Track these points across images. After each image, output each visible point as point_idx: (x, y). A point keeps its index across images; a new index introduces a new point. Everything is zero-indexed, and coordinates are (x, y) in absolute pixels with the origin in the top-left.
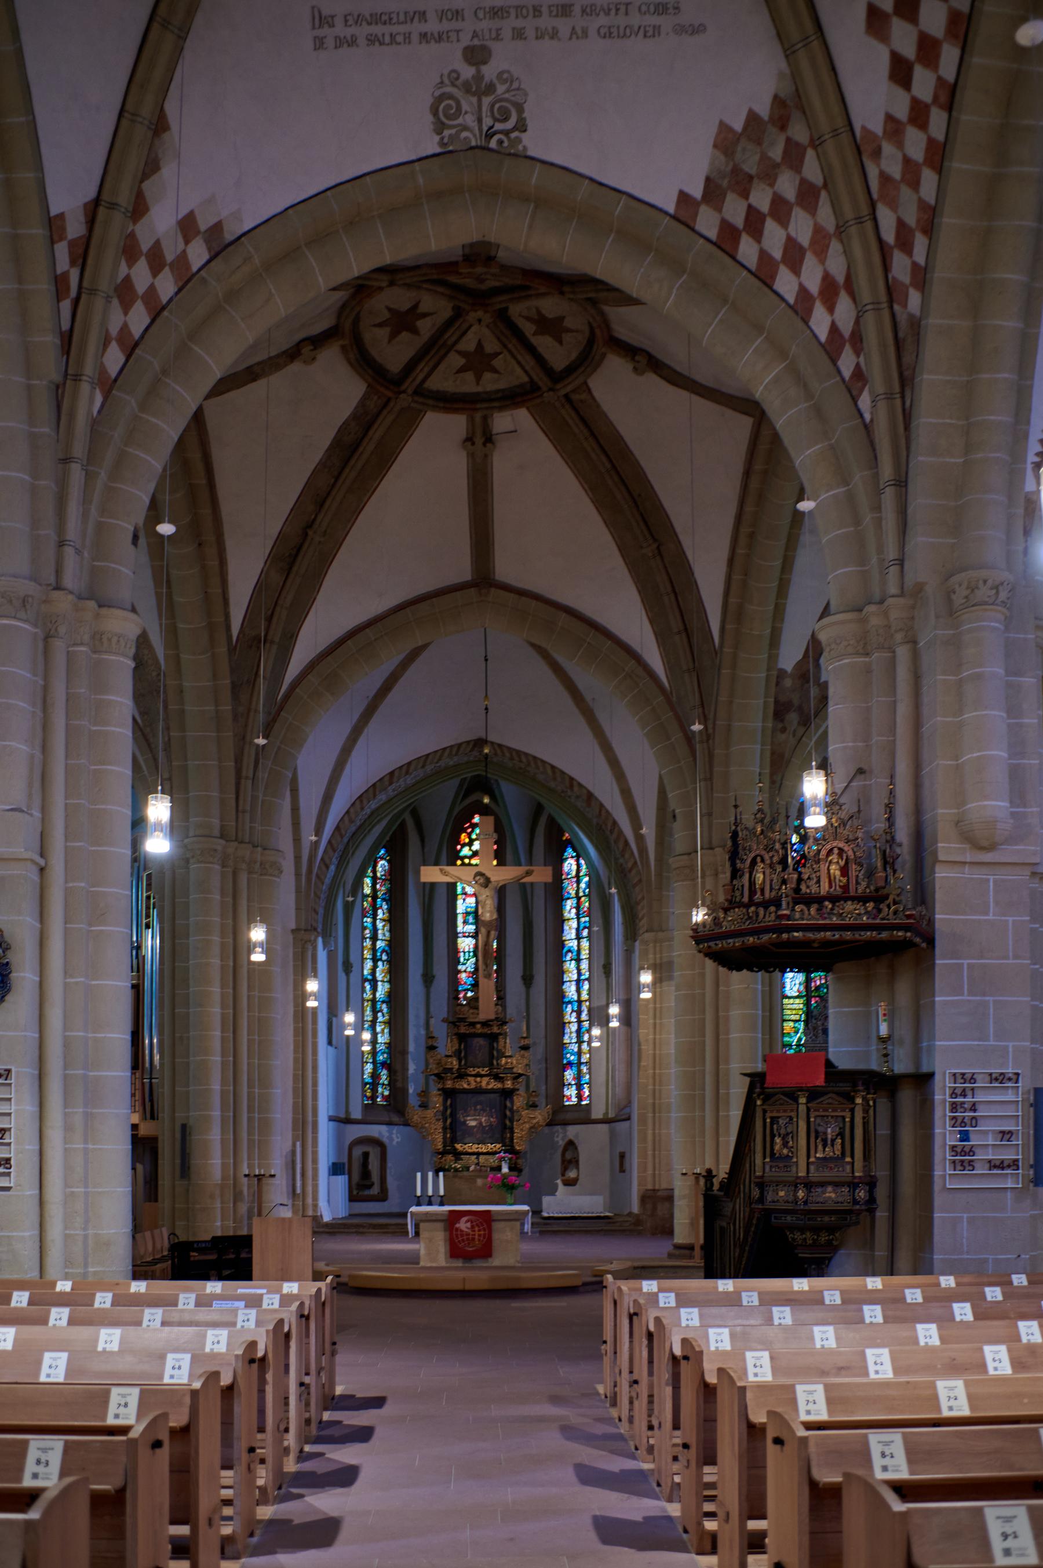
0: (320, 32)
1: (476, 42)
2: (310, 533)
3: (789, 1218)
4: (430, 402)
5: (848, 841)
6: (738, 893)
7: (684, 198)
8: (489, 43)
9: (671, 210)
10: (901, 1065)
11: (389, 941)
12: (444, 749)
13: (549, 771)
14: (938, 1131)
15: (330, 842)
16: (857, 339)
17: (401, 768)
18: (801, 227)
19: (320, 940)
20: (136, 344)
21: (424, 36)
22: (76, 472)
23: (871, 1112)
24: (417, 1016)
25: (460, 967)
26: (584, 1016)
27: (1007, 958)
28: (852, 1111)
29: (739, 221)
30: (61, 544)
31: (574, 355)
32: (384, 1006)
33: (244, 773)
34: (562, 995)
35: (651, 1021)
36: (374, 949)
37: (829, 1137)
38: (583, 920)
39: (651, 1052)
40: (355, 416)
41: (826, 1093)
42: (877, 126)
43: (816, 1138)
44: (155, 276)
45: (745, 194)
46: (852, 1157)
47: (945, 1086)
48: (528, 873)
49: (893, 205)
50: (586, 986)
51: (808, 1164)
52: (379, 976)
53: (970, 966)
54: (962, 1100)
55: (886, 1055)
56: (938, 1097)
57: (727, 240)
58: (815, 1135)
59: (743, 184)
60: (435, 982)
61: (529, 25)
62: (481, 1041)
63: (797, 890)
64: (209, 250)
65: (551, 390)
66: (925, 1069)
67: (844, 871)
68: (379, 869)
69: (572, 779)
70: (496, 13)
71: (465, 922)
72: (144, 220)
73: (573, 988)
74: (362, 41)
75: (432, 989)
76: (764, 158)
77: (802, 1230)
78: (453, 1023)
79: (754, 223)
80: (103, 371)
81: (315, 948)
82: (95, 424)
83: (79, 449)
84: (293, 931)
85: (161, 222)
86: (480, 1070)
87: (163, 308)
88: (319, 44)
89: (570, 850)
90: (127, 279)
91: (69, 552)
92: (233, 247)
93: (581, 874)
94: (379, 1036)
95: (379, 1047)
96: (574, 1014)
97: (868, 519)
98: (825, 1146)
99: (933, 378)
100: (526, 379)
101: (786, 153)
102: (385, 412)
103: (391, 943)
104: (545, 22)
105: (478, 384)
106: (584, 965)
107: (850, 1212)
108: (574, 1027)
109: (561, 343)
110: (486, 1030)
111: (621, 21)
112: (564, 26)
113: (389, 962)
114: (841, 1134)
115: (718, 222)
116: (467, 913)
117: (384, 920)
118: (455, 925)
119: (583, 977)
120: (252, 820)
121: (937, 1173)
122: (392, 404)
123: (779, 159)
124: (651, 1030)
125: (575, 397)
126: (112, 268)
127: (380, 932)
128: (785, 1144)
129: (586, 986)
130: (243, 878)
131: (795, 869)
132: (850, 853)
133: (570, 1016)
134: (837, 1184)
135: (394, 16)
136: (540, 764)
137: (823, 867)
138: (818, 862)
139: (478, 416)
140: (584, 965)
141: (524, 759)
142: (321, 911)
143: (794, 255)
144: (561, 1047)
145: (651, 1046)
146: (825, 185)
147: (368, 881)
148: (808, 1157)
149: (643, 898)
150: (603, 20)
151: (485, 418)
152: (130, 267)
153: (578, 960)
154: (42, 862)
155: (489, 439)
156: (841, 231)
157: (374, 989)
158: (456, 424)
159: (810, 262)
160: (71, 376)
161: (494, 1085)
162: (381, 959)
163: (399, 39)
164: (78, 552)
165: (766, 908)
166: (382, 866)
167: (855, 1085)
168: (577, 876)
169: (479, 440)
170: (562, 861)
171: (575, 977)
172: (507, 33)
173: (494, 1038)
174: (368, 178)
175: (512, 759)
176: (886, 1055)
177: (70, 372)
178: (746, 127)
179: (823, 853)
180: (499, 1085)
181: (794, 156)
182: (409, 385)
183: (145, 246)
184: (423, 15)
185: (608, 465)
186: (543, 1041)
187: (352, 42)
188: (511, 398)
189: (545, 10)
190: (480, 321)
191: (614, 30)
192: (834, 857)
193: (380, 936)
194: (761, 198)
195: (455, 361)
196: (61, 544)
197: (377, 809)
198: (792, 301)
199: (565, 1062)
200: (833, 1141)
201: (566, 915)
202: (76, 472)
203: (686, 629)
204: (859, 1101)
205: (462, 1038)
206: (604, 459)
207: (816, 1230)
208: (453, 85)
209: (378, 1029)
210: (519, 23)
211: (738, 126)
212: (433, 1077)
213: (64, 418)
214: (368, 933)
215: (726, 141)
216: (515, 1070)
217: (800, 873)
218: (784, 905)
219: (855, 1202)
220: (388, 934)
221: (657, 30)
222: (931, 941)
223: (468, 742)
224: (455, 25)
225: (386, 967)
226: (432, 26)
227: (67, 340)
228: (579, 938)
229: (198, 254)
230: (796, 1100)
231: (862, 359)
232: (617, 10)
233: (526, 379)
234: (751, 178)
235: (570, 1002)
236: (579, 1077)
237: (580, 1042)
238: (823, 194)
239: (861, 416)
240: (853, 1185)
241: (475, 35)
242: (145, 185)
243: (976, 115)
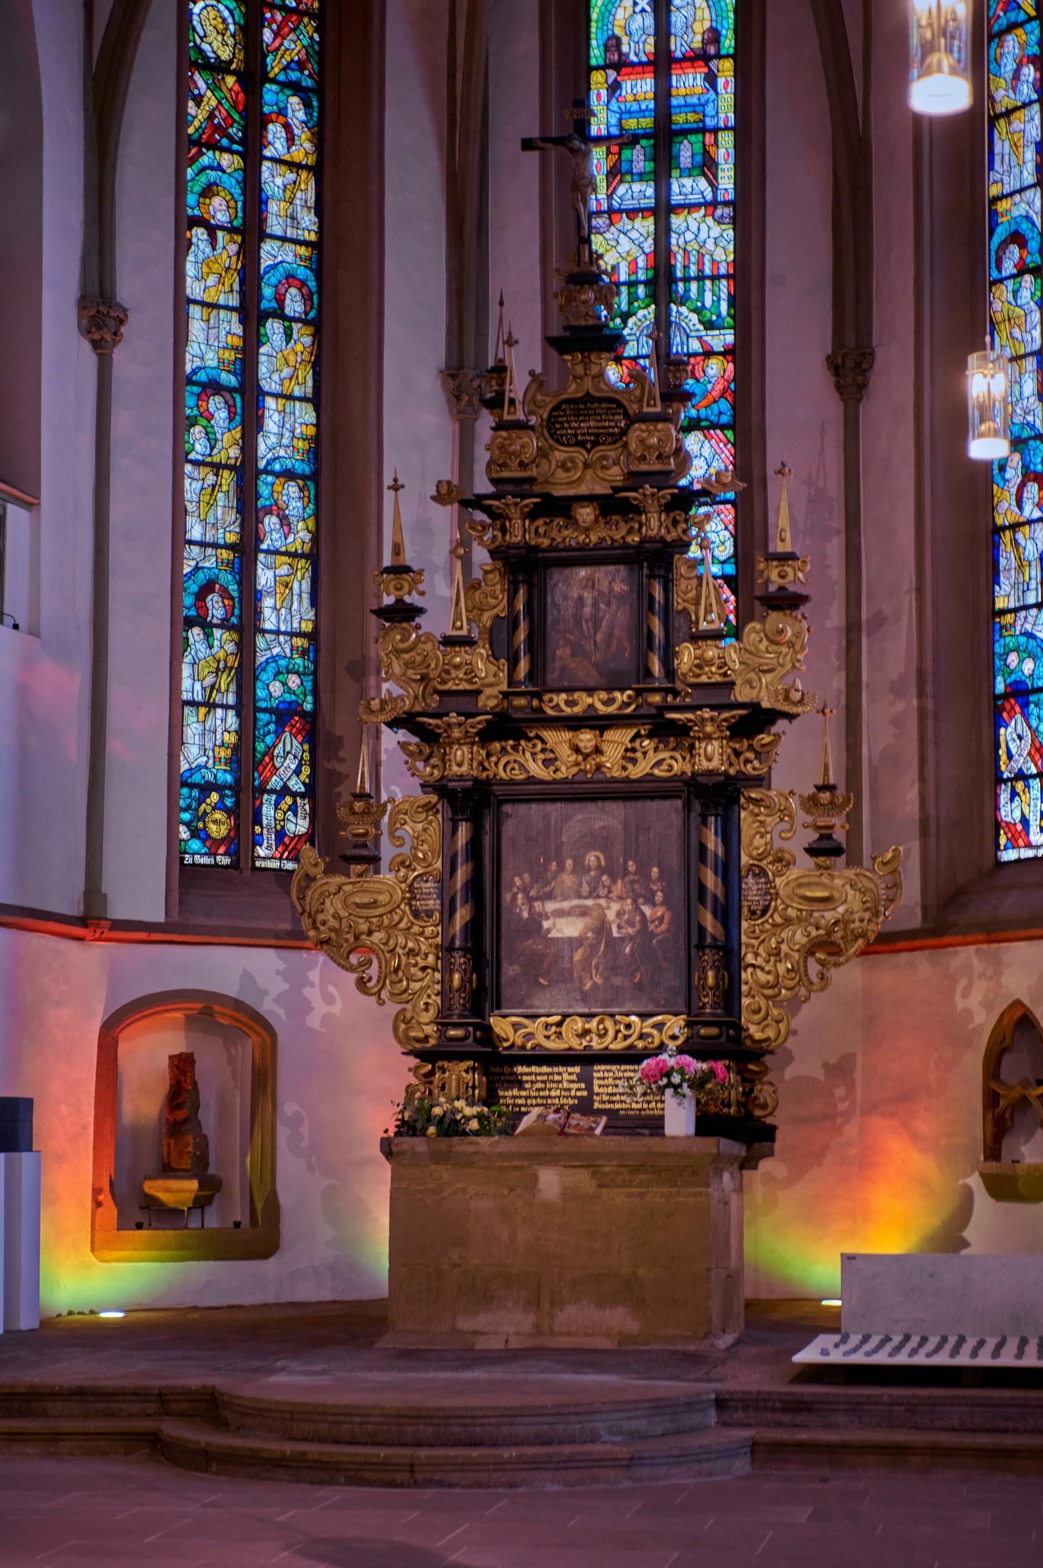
32: (292, 489)
36: (249, 274)
52: (270, 374)
71: (615, 173)
86: (585, 700)
94: (268, 602)
103: (321, 252)
110: (619, 532)
117: (292, 165)
127: (273, 207)
157: (251, 423)
161: (656, 761)
162: (279, 313)
180: (679, 766)
186: (908, 603)
193: (275, 225)
199: (1000, 688)
205: (525, 568)
209: (264, 577)
212: (402, 735)
216: (742, 694)
220: (308, 220)
225: (303, 338)
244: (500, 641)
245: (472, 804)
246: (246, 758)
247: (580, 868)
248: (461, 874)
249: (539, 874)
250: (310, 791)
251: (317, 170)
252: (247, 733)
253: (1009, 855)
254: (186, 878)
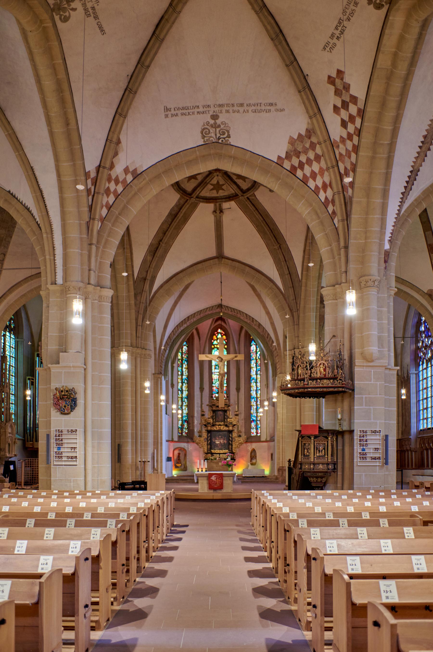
0: (167, 113)
1: (214, 114)
2: (161, 243)
3: (309, 474)
4: (201, 200)
5: (326, 361)
6: (294, 376)
7: (279, 158)
8: (218, 114)
9: (276, 161)
10: (345, 427)
11: (188, 376)
12: (207, 308)
13: (245, 315)
14: (355, 448)
15: (166, 342)
16: (333, 202)
17: (192, 315)
18: (316, 167)
19: (163, 377)
20: (111, 207)
21: (198, 112)
22: (94, 247)
23: (335, 442)
24: (198, 403)
25: (213, 385)
26: (258, 403)
27: (377, 395)
28: (328, 442)
29: (297, 165)
30: (90, 270)
31: (250, 185)
32: (186, 399)
33: (139, 324)
34: (250, 395)
35: (282, 406)
36: (182, 379)
38: (258, 368)
39: (281, 417)
40: (176, 205)
41: (320, 436)
42: (338, 139)
44: (116, 186)
45: (298, 157)
46: (328, 455)
48: (236, 357)
49: (343, 162)
50: (259, 392)
52: (184, 388)
53: (366, 398)
54: (363, 438)
55: (340, 424)
56: (355, 437)
57: (293, 171)
58: (316, 449)
59: (298, 154)
60: (204, 390)
61: (231, 109)
62: (221, 413)
63: (310, 376)
64: (133, 176)
65: (242, 196)
66: (352, 429)
67: (325, 370)
68: (184, 349)
69: (253, 318)
70: (220, 106)
71: (215, 368)
72: (113, 170)
73: (255, 393)
74: (179, 115)
75: (203, 393)
76: (304, 146)
77: (313, 477)
78: (211, 406)
79: (301, 166)
80: (101, 215)
81: (161, 380)
82: (99, 232)
83: (94, 241)
84: (153, 374)
85: (118, 170)
86: (219, 423)
87: (119, 195)
88: (167, 116)
89: (253, 342)
90: (108, 188)
91: (92, 272)
92: (140, 176)
93: (258, 351)
95: (184, 415)
96: (255, 402)
97: (337, 257)
99: (355, 217)
100: (234, 192)
101: (310, 146)
102: (186, 204)
104: (236, 108)
105: (217, 194)
106: (259, 384)
107: (327, 472)
108: (255, 407)
109: (245, 182)
111: (259, 108)
112: (241, 109)
113: (187, 383)
114: (324, 449)
115: (290, 165)
116: (216, 365)
117: (185, 368)
118: (211, 370)
119: (258, 389)
120: (141, 340)
121: (355, 460)
122: (188, 201)
123: (308, 147)
124: (282, 409)
125: (250, 198)
126: (104, 184)
127: (184, 372)
128: (308, 452)
129: (259, 392)
130: (138, 360)
131: (310, 369)
132: (326, 365)
133: (253, 403)
134: (323, 464)
135: (189, 107)
136: (241, 313)
137: (318, 369)
138: (317, 367)
139: (218, 204)
140: (259, 384)
141: (236, 311)
142: (163, 367)
143: (314, 176)
144: (250, 414)
145: (281, 415)
146: (322, 156)
147: (180, 354)
148: (314, 455)
149: (279, 361)
150: (253, 108)
151: (220, 205)
152: (109, 184)
153: (256, 383)
154: (85, 367)
155: (221, 211)
156: (328, 169)
158: (211, 206)
159: (318, 178)
160: (92, 218)
161: (226, 428)
163: (191, 113)
164: (94, 272)
165: (300, 381)
166: (185, 348)
167: (328, 434)
168: (256, 352)
169: (218, 212)
170: (251, 346)
171: (255, 389)
172: (224, 111)
173: (225, 411)
174: (181, 153)
175: (231, 311)
176: (340, 424)
177: (92, 217)
178: (298, 137)
179: (318, 365)
180: (227, 429)
181: (313, 146)
182: (194, 195)
183: (113, 177)
184: (198, 107)
185: (262, 219)
186: (243, 412)
187: (177, 115)
188: (229, 198)
189: (235, 105)
190: (218, 175)
191: (257, 111)
192: (322, 366)
193: (184, 374)
194: (303, 158)
195: (210, 187)
196: (90, 270)
197: (183, 330)
198: (313, 189)
200: (322, 451)
201: (252, 366)
202: (94, 247)
203: (290, 273)
204: (330, 439)
205: (214, 411)
206: (261, 217)
207: (317, 477)
208: (207, 125)
209: (184, 408)
210: (228, 108)
211: (296, 137)
213: (90, 231)
214: (180, 373)
215: (292, 141)
217: (311, 371)
218: (306, 381)
219: (328, 469)
220: (187, 373)
221: (270, 111)
222: (353, 390)
223: (216, 306)
224: (208, 109)
225: (186, 385)
226: (201, 109)
227: (91, 208)
228: (256, 374)
229: (129, 178)
230: (310, 438)
231: (335, 208)
232: (257, 105)
233: (234, 192)
234: (300, 152)
235: (253, 398)
236: (256, 425)
237: (257, 412)
238: (322, 157)
239: (335, 225)
240: (328, 464)
241: (214, 112)
242: (114, 160)
243: (367, 138)
244: (212, 417)
245: (209, 432)
246: (182, 425)
247: (219, 437)
248: (209, 438)
249: (215, 438)
250: (188, 428)
251: (188, 369)
252: (182, 423)
253: (252, 435)
254: (179, 437)
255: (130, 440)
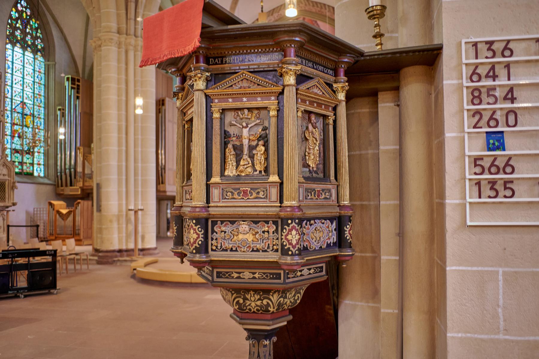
37: (246, 142)
43: (225, 145)
46: (280, 174)
47: (460, 64)
51: (208, 187)
54: (490, 83)
66: (436, 42)
98: (238, 158)
114: (264, 138)
134: (255, 220)
148: (209, 176)
200: (252, 148)
255: (114, 176)
